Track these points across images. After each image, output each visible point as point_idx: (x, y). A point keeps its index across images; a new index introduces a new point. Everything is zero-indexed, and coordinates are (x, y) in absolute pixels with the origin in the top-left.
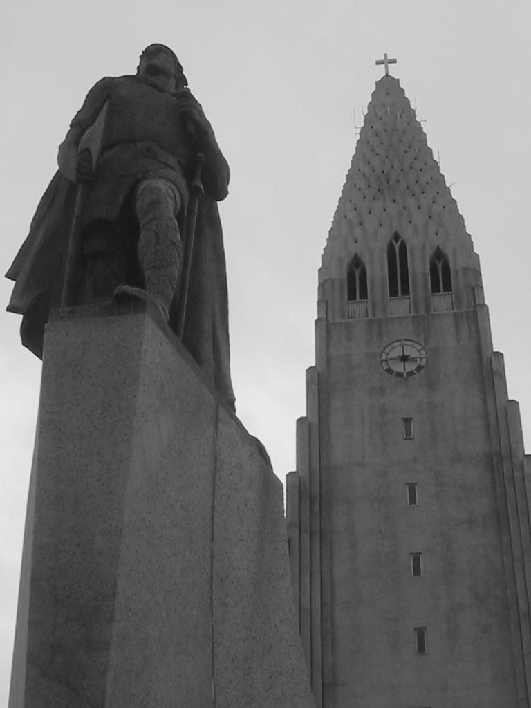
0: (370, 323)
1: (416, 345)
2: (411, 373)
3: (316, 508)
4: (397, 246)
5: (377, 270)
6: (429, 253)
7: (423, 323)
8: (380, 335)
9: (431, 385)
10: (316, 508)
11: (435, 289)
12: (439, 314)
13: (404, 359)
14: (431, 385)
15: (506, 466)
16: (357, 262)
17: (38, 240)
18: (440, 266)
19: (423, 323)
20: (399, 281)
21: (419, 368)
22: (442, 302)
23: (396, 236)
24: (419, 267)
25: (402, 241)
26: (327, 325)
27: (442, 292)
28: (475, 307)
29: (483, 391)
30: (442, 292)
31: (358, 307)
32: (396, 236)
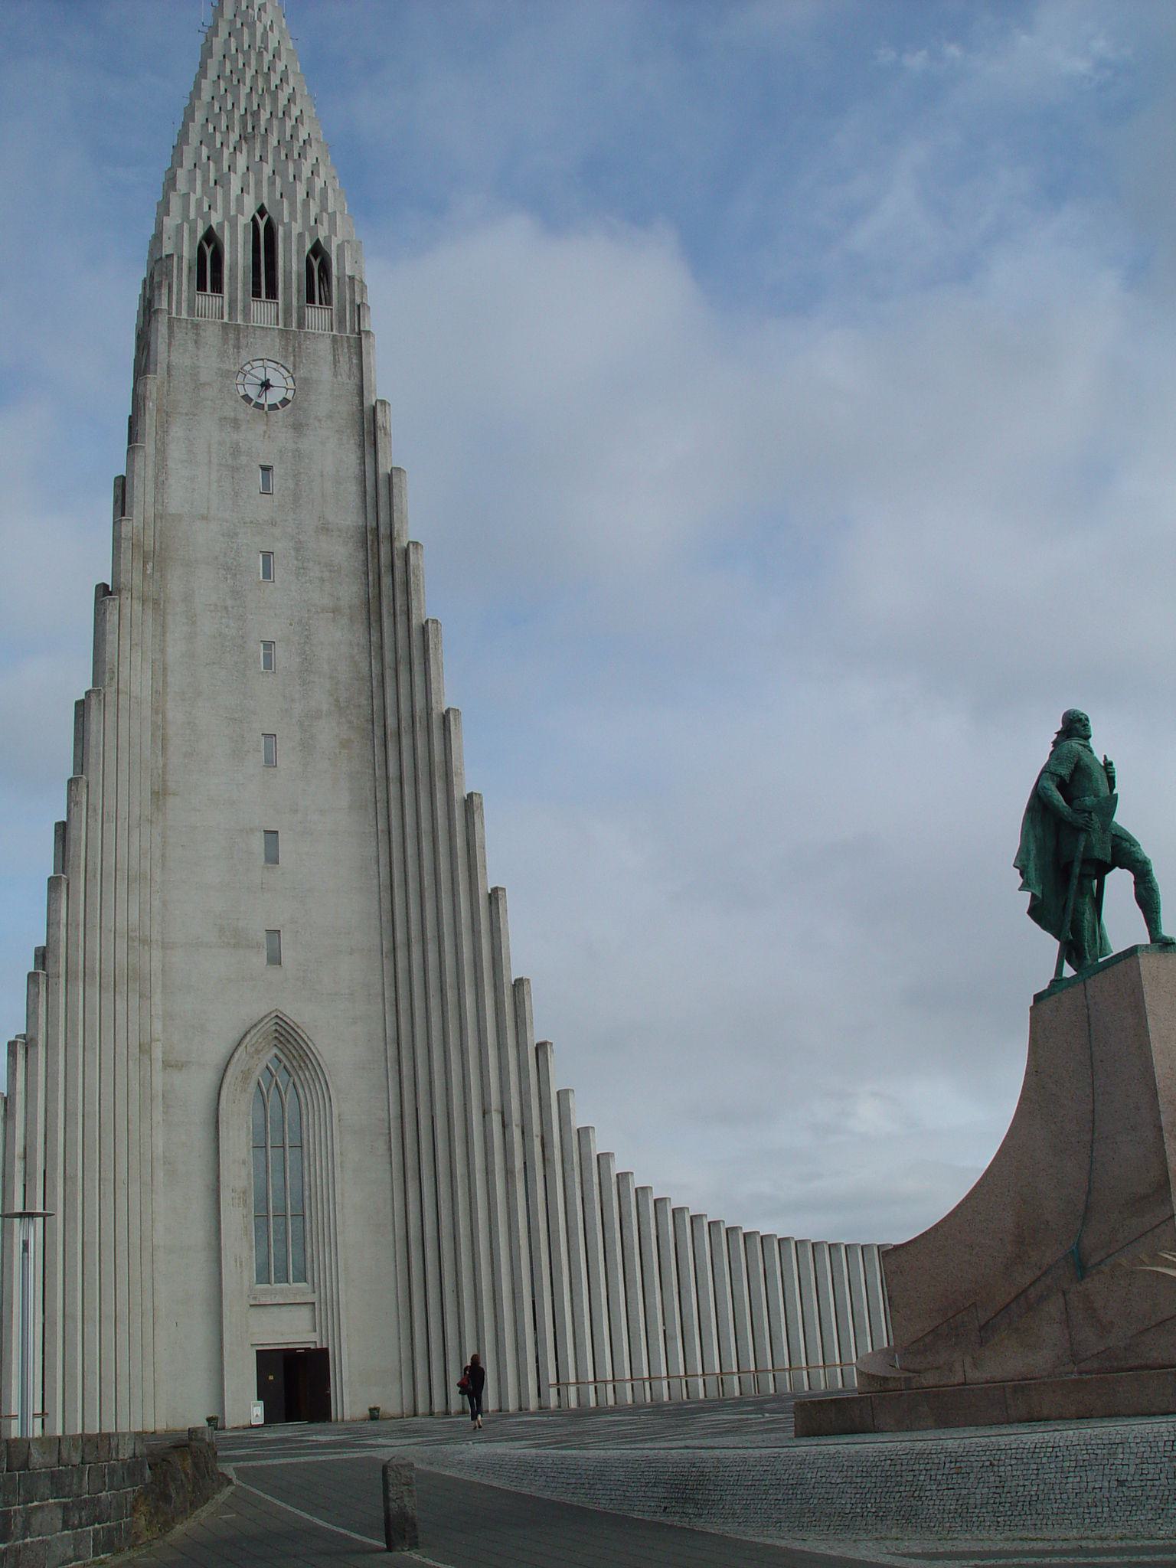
0: (225, 326)
1: (282, 370)
4: (262, 224)
5: (237, 255)
7: (293, 336)
8: (237, 347)
9: (298, 428)
12: (314, 334)
14: (298, 428)
15: (384, 549)
16: (210, 237)
17: (1033, 847)
19: (293, 336)
21: (285, 402)
22: (316, 316)
24: (291, 263)
25: (269, 218)
26: (169, 318)
27: (317, 304)
28: (359, 333)
29: (362, 446)
30: (317, 304)
31: (207, 301)
32: (262, 211)
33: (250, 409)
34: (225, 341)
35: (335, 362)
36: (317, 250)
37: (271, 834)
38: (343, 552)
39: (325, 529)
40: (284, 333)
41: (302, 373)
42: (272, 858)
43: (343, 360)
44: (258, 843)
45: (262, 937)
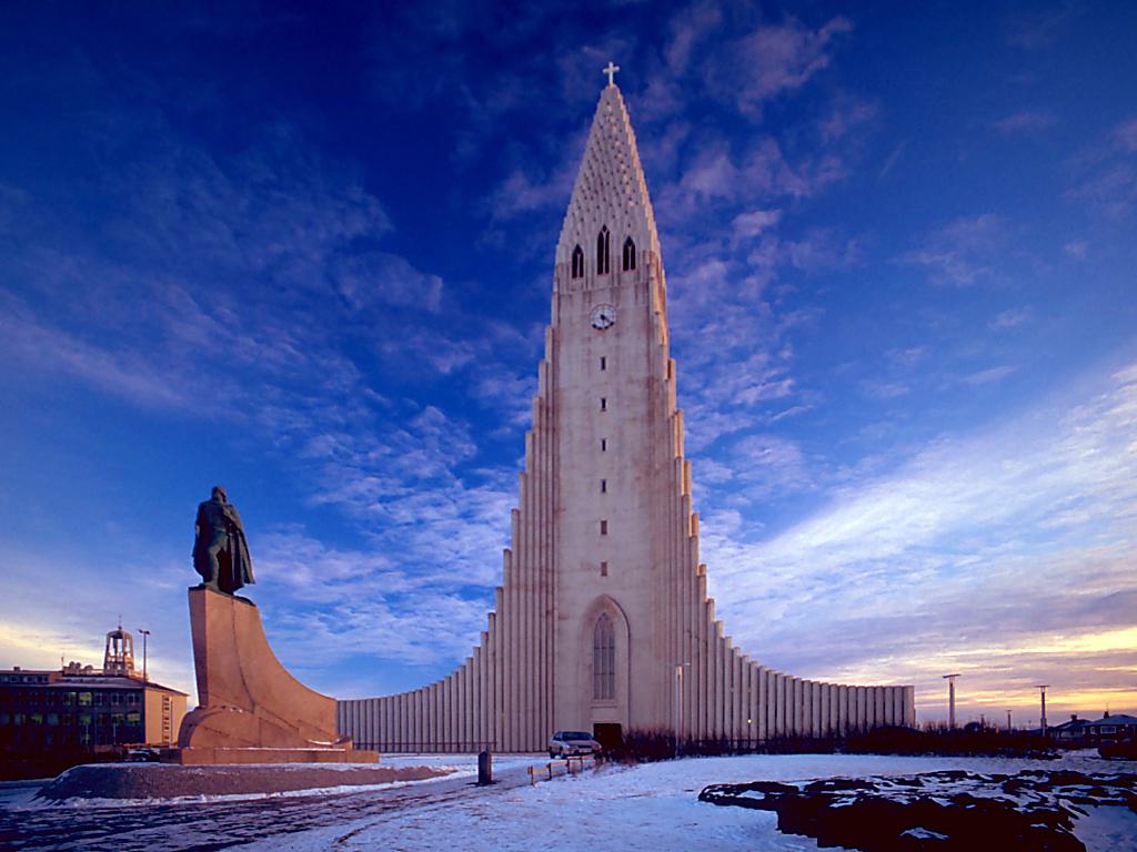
0: (584, 294)
2: (607, 328)
3: (550, 414)
5: (590, 255)
6: (623, 241)
7: (616, 292)
8: (590, 302)
10: (550, 414)
11: (626, 268)
13: (603, 317)
14: (618, 335)
16: (578, 250)
18: (630, 248)
19: (616, 292)
20: (603, 265)
22: (629, 276)
23: (605, 228)
24: (616, 251)
31: (578, 282)
33: (596, 331)
34: (584, 299)
35: (636, 297)
36: (629, 242)
37: (604, 524)
38: (638, 391)
39: (631, 381)
40: (612, 290)
41: (620, 307)
42: (604, 532)
43: (640, 295)
44: (599, 526)
45: (600, 565)
